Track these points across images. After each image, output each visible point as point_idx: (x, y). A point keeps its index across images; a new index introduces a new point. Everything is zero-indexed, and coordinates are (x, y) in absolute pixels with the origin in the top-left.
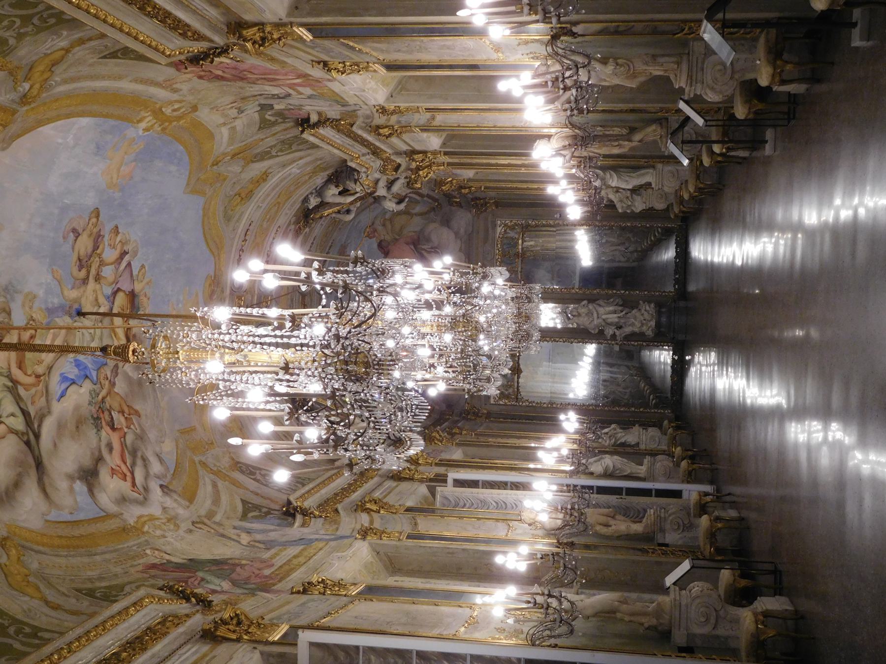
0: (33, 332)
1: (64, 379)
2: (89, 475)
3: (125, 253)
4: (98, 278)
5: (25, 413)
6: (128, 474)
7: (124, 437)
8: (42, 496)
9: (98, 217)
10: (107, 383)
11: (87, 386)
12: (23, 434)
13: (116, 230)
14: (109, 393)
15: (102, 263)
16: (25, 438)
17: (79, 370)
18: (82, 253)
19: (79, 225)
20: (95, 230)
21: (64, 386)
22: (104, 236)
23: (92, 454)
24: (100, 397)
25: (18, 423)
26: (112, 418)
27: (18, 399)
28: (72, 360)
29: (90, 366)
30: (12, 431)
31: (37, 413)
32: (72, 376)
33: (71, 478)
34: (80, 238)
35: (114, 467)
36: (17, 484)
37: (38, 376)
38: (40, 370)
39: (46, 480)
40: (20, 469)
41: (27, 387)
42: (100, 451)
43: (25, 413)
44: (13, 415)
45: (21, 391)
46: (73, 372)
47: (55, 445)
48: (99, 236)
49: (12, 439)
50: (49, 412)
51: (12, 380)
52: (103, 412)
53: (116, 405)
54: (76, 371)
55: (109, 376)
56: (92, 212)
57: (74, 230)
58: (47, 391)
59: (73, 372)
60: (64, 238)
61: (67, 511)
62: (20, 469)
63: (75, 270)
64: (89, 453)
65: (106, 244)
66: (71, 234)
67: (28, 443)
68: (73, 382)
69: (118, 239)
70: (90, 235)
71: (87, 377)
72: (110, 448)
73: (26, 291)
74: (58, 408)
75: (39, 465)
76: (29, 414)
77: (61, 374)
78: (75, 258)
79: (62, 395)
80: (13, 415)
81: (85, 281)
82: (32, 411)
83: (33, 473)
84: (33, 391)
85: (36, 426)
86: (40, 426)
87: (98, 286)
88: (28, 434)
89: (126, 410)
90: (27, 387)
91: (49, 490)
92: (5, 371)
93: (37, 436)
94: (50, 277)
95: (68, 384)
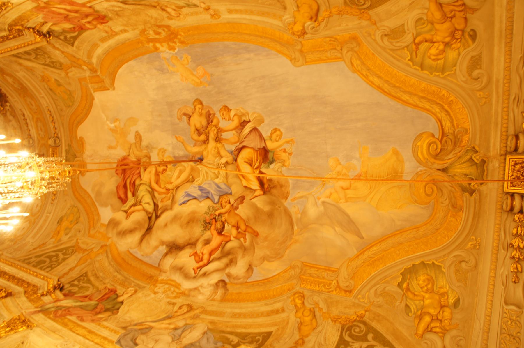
0: (165, 167)
1: (188, 195)
2: (174, 248)
3: (243, 124)
4: (218, 139)
5: (156, 205)
6: (205, 261)
7: (227, 242)
8: (139, 241)
9: (201, 103)
10: (228, 206)
11: (208, 203)
12: (150, 213)
13: (227, 109)
14: (229, 212)
15: (220, 131)
16: (150, 215)
17: (202, 193)
18: (198, 126)
19: (189, 111)
20: (204, 112)
21: (186, 199)
22: (214, 114)
23: (190, 239)
24: (218, 212)
25: (150, 208)
26: (224, 227)
27: (153, 198)
28: (197, 186)
29: (213, 192)
30: (144, 210)
31: (162, 207)
32: (196, 195)
33: (163, 243)
34: (191, 118)
35: (198, 252)
36: (131, 231)
37: (168, 190)
38: (170, 187)
39: (147, 237)
40: (138, 227)
41: (160, 193)
42: (197, 240)
43: (156, 205)
44: (148, 203)
45: (156, 194)
46: (197, 193)
47: (166, 225)
48: (210, 114)
49: (143, 214)
50: (171, 209)
51: (151, 188)
52: (216, 221)
53: (233, 221)
54: (199, 193)
55: (232, 202)
56: (194, 102)
57: (185, 114)
58: (173, 197)
59: (197, 193)
60: (179, 119)
61: (142, 253)
62: (138, 227)
63: (196, 137)
64: (187, 238)
65: (220, 119)
66: (185, 118)
67: (150, 218)
68: (195, 198)
69: (232, 114)
70: (201, 115)
71: (208, 198)
72: (207, 242)
73: (160, 147)
74: (177, 209)
75: (149, 229)
76: (158, 206)
77: (186, 192)
78: (193, 129)
79: (184, 203)
80: (148, 203)
81: (206, 141)
82: (160, 205)
83: (143, 231)
84: (164, 196)
85: (159, 212)
86: (162, 213)
87: (219, 145)
88: (152, 214)
89: (243, 227)
90: (160, 193)
91: (145, 241)
92: (148, 183)
93: (157, 217)
94: (175, 141)
95: (191, 198)
